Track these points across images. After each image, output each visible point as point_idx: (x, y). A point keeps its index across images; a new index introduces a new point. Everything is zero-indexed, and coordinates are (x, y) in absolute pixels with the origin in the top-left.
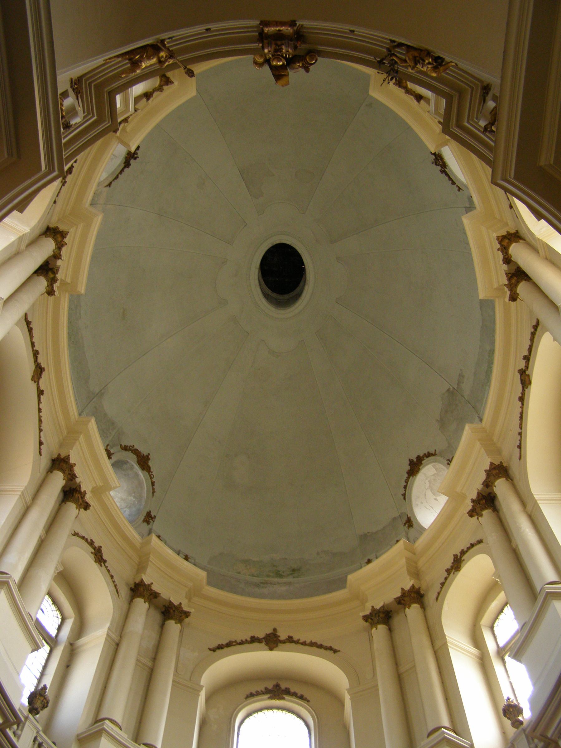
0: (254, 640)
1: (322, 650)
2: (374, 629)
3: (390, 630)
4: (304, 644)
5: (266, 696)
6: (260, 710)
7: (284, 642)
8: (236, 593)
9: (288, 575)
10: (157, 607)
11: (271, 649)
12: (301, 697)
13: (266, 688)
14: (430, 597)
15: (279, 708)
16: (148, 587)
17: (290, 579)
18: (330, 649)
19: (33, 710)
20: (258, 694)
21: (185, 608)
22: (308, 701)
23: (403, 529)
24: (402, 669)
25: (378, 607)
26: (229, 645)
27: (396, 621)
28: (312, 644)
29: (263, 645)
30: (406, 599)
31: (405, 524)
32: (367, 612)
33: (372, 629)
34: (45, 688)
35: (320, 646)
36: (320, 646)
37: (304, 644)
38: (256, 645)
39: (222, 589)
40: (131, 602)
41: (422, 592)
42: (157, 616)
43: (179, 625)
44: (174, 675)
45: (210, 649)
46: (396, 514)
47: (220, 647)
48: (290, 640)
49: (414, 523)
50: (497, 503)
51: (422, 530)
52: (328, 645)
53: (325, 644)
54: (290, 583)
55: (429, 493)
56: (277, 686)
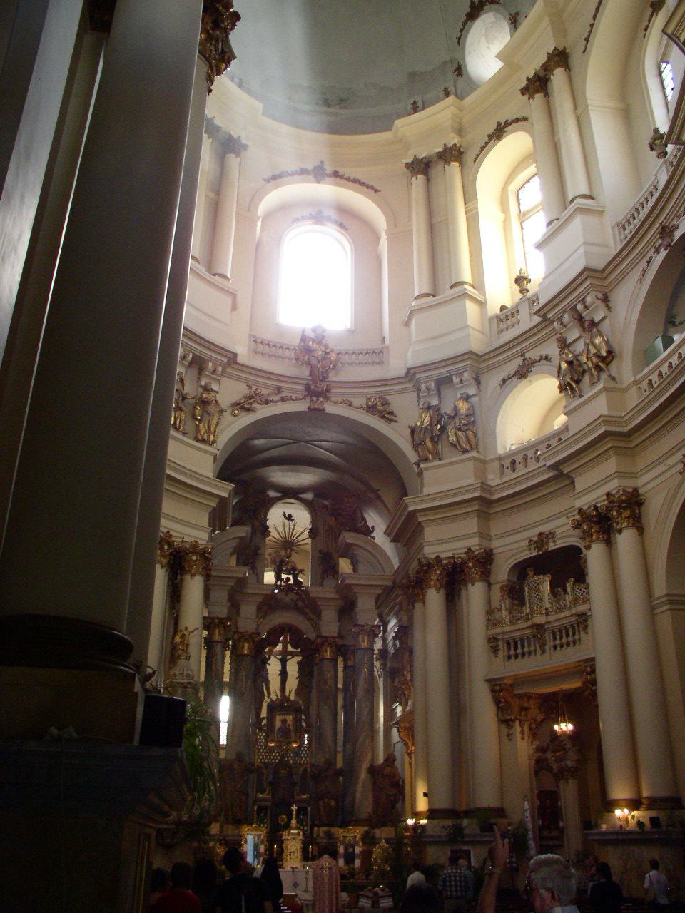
1: (364, 189)
2: (414, 178)
3: (428, 180)
5: (310, 222)
9: (336, 105)
11: (318, 182)
13: (310, 214)
14: (469, 157)
20: (304, 218)
21: (244, 141)
22: (347, 230)
23: (451, 76)
24: (434, 221)
27: (436, 170)
28: (356, 181)
29: (311, 177)
30: (447, 155)
31: (455, 71)
32: (410, 160)
33: (412, 177)
35: (363, 184)
37: (348, 179)
38: (304, 176)
41: (462, 150)
43: (238, 158)
44: (237, 208)
45: (264, 180)
46: (448, 59)
49: (464, 72)
50: (549, 85)
51: (473, 85)
52: (371, 183)
53: (367, 182)
55: (483, 40)
56: (320, 212)
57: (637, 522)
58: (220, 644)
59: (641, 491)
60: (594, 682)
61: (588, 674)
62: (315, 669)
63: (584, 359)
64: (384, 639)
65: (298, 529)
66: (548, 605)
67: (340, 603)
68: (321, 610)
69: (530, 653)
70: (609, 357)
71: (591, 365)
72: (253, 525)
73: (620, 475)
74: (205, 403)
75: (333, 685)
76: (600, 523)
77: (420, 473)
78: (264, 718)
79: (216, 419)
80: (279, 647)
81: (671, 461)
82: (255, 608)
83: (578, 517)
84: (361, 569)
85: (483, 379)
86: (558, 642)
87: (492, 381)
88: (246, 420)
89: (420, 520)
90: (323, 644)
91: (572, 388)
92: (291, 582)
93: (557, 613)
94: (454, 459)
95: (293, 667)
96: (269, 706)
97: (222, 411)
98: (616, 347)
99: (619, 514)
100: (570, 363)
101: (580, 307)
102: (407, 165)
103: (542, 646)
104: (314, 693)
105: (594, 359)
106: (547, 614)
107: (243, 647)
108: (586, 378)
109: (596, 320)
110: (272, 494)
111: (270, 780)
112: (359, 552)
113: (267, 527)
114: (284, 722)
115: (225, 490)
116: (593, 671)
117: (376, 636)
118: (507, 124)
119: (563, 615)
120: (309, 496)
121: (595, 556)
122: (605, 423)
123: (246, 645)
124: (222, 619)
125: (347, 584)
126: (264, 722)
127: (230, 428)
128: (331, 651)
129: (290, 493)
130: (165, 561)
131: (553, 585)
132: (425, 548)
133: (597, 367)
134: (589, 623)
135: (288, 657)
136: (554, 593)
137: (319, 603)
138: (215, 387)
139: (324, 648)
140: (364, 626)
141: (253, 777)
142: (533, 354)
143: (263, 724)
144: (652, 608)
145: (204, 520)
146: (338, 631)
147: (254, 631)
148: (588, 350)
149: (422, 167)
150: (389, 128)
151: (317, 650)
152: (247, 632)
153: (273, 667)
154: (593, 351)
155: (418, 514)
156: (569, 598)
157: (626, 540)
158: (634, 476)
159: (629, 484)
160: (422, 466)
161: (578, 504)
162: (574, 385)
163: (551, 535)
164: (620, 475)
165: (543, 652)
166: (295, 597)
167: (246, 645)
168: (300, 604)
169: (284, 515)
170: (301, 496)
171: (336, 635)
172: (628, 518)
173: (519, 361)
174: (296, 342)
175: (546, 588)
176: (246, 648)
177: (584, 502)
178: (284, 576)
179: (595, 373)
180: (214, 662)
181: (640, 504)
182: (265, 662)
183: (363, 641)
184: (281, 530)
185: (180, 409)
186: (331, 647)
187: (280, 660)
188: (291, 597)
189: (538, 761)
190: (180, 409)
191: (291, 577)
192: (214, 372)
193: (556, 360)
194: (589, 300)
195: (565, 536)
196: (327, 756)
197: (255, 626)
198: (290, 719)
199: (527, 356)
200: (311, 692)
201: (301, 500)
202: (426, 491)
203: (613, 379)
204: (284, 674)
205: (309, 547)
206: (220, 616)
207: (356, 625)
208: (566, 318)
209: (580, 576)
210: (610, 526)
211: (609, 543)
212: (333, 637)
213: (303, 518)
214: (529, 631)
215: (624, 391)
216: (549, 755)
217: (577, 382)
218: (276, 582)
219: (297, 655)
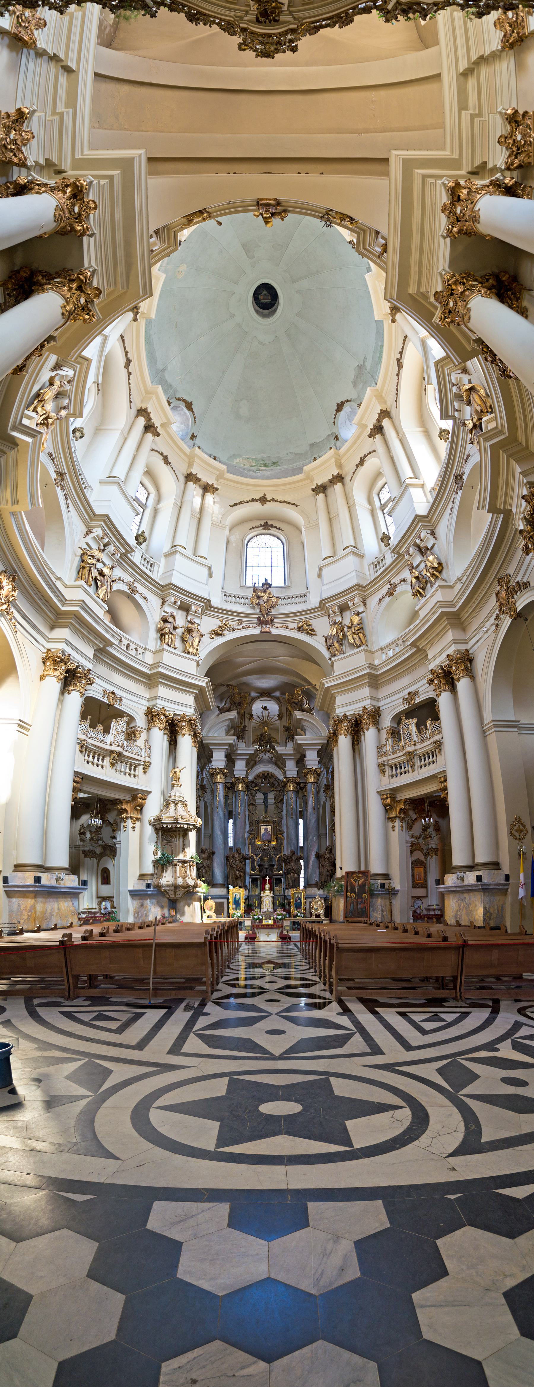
0: (253, 500)
4: (280, 502)
6: (258, 535)
7: (269, 501)
8: (242, 476)
10: (200, 486)
12: (279, 529)
15: (268, 534)
16: (195, 476)
17: (272, 468)
18: (294, 504)
19: (139, 544)
20: (256, 527)
21: (216, 486)
25: (319, 484)
26: (240, 503)
27: (329, 491)
28: (285, 502)
34: (143, 532)
35: (289, 503)
36: (289, 503)
37: (280, 502)
38: (255, 503)
39: (235, 474)
40: (186, 484)
42: (200, 491)
47: (236, 504)
48: (273, 500)
54: (272, 470)
57: (470, 673)
59: (471, 652)
60: (445, 789)
61: (441, 782)
63: (424, 572)
64: (327, 778)
65: (272, 715)
66: (415, 738)
67: (298, 756)
69: (405, 773)
70: (439, 568)
71: (429, 574)
72: (238, 713)
73: (455, 641)
74: (190, 631)
76: (446, 678)
79: (196, 641)
81: (488, 625)
82: (244, 763)
83: (431, 676)
84: (308, 735)
85: (368, 602)
86: (423, 763)
87: (373, 601)
88: (220, 641)
91: (420, 594)
93: (421, 743)
94: (352, 652)
97: (202, 636)
98: (443, 562)
99: (457, 668)
100: (417, 578)
101: (418, 541)
102: (313, 490)
103: (413, 766)
104: (284, 812)
105: (431, 571)
106: (415, 745)
108: (429, 585)
109: (429, 547)
112: (305, 724)
113: (252, 715)
114: (266, 830)
115: (203, 682)
116: (446, 780)
117: (319, 775)
118: (365, 456)
119: (425, 744)
120: (277, 694)
121: (444, 701)
122: (442, 606)
123: (240, 785)
127: (207, 647)
129: (265, 693)
130: (162, 726)
131: (418, 725)
133: (433, 575)
134: (442, 746)
136: (419, 730)
138: (197, 621)
141: (248, 861)
142: (396, 580)
144: (484, 732)
145: (189, 700)
148: (426, 566)
149: (322, 489)
150: (302, 473)
151: (285, 786)
154: (429, 564)
156: (429, 732)
157: (463, 685)
158: (466, 642)
159: (463, 647)
161: (431, 667)
162: (421, 591)
163: (416, 693)
164: (455, 641)
165: (413, 771)
166: (270, 756)
167: (240, 785)
170: (274, 694)
172: (463, 670)
173: (388, 586)
174: (250, 593)
175: (414, 728)
176: (240, 787)
177: (433, 665)
179: (433, 580)
181: (471, 661)
185: (171, 633)
188: (268, 755)
189: (413, 844)
190: (171, 633)
192: (196, 612)
193: (409, 582)
194: (422, 535)
195: (425, 692)
197: (245, 773)
198: (269, 828)
199: (392, 582)
203: (444, 580)
205: (279, 725)
208: (411, 550)
209: (436, 717)
210: (453, 679)
211: (453, 689)
213: (274, 707)
214: (403, 758)
215: (452, 587)
216: (421, 841)
217: (423, 589)
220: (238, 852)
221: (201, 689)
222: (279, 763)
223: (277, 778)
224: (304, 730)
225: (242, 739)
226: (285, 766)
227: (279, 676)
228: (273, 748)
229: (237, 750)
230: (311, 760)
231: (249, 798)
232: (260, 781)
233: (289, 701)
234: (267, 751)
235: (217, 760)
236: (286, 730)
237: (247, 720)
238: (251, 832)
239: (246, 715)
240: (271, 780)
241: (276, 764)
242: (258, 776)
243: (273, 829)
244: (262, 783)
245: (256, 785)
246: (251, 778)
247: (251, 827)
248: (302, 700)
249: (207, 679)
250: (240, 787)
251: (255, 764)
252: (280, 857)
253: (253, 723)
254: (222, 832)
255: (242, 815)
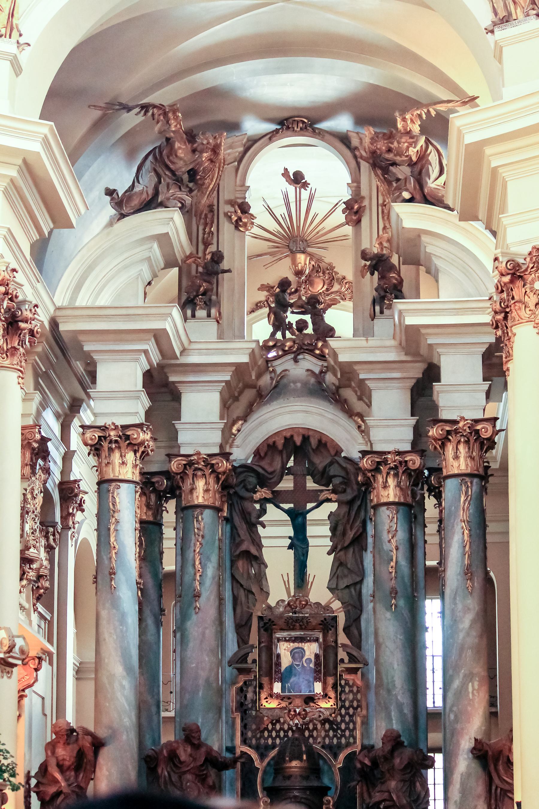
58: (123, 486)
62: (370, 530)
65: (320, 208)
67: (416, 371)
68: (370, 391)
75: (404, 563)
77: (499, 55)
78: (252, 647)
80: (287, 484)
84: (448, 292)
89: (493, 165)
90: (377, 470)
92: (310, 330)
95: (319, 534)
96: (260, 618)
107: (192, 490)
110: (253, 126)
111: (269, 782)
113: (244, 208)
120: (343, 123)
124: (125, 427)
125: (408, 327)
126: (254, 655)
128: (398, 485)
129: (295, 122)
132: (509, 230)
135: (309, 506)
137: (362, 376)
139: (380, 479)
140: (455, 422)
143: (250, 660)
146: (409, 435)
147: (216, 450)
151: (368, 486)
152: (198, 454)
153: (274, 530)
155: (488, 151)
160: (499, 33)
166: (315, 365)
167: (200, 484)
168: (330, 378)
169: (286, 173)
171: (407, 447)
176: (201, 491)
178: (292, 318)
180: (112, 527)
182: (252, 523)
183: (456, 457)
184: (280, 211)
186: (396, 475)
187: (288, 512)
188: (309, 363)
191: (308, 318)
196: (396, 726)
197: (216, 437)
200: (361, 582)
201: (320, 134)
202: (508, 93)
204: (299, 544)
206: (120, 422)
207: (437, 421)
212: (399, 453)
213: (330, 176)
218: (273, 334)
219: (328, 500)
220: (191, 736)
221: (29, 168)
222: (348, 394)
223: (338, 451)
224: (433, 274)
225: (208, 305)
226: (369, 405)
227: (340, 64)
228: (326, 332)
229: (184, 351)
230: (456, 387)
231: (234, 528)
232: (277, 465)
233: (381, 165)
234: (303, 348)
235: (112, 395)
236: (373, 269)
237: (227, 228)
238: (240, 662)
239: (225, 208)
240: (320, 462)
241: (335, 397)
242: (268, 449)
243: (329, 649)
244: (284, 471)
245: (263, 481)
246: (242, 453)
247: (243, 640)
248: (423, 157)
249: (46, 128)
250: (201, 491)
251: (262, 397)
252: (351, 758)
253: (250, 242)
254: (128, 669)
255: (207, 601)
